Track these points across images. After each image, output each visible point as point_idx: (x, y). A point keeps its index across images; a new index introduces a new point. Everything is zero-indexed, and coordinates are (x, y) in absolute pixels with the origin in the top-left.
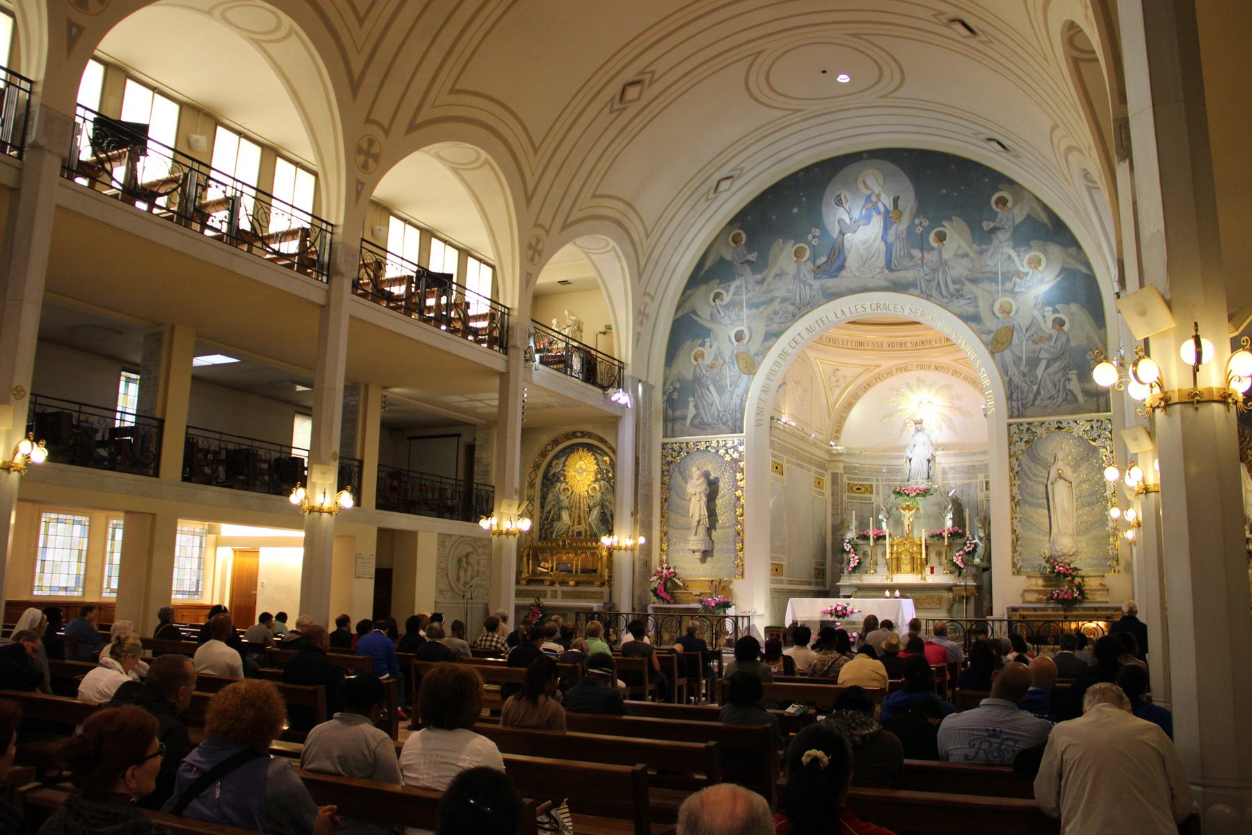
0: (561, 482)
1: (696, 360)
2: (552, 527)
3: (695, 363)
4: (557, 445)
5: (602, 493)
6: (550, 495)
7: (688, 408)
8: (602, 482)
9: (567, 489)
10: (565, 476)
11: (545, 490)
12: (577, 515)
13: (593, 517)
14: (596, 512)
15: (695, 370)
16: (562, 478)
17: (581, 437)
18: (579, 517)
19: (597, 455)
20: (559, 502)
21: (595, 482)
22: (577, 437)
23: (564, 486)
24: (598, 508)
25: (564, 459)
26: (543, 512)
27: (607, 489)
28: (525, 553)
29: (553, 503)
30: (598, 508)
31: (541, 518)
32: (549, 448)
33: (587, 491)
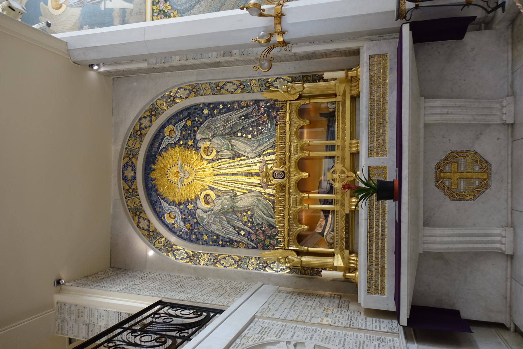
0: (196, 208)
1: (61, 6)
2: (260, 225)
3: (64, 6)
4: (142, 211)
5: (213, 136)
6: (214, 228)
7: (112, 10)
8: (199, 136)
9: (207, 195)
10: (188, 202)
11: (205, 237)
12: (246, 179)
13: (249, 149)
14: (240, 145)
15: (71, 6)
16: (190, 207)
17: (134, 169)
18: (247, 175)
19: (163, 146)
20: (224, 212)
21: (197, 149)
22: (134, 178)
23: (201, 204)
24: (235, 142)
25: (164, 204)
26: (238, 242)
27: (208, 128)
28: (295, 258)
29: (225, 223)
30: (235, 142)
31: (247, 246)
32: (144, 224)
33: (213, 160)
